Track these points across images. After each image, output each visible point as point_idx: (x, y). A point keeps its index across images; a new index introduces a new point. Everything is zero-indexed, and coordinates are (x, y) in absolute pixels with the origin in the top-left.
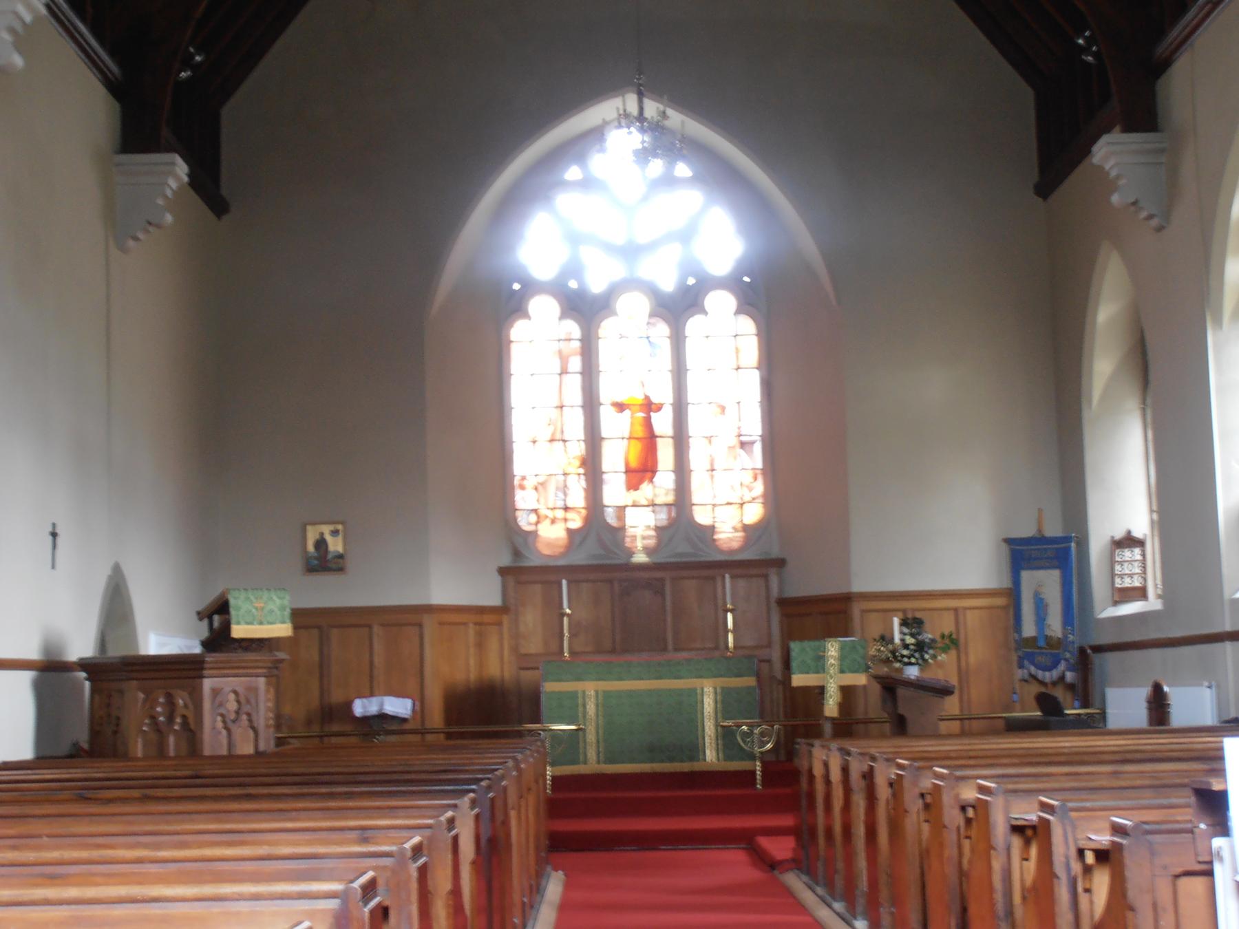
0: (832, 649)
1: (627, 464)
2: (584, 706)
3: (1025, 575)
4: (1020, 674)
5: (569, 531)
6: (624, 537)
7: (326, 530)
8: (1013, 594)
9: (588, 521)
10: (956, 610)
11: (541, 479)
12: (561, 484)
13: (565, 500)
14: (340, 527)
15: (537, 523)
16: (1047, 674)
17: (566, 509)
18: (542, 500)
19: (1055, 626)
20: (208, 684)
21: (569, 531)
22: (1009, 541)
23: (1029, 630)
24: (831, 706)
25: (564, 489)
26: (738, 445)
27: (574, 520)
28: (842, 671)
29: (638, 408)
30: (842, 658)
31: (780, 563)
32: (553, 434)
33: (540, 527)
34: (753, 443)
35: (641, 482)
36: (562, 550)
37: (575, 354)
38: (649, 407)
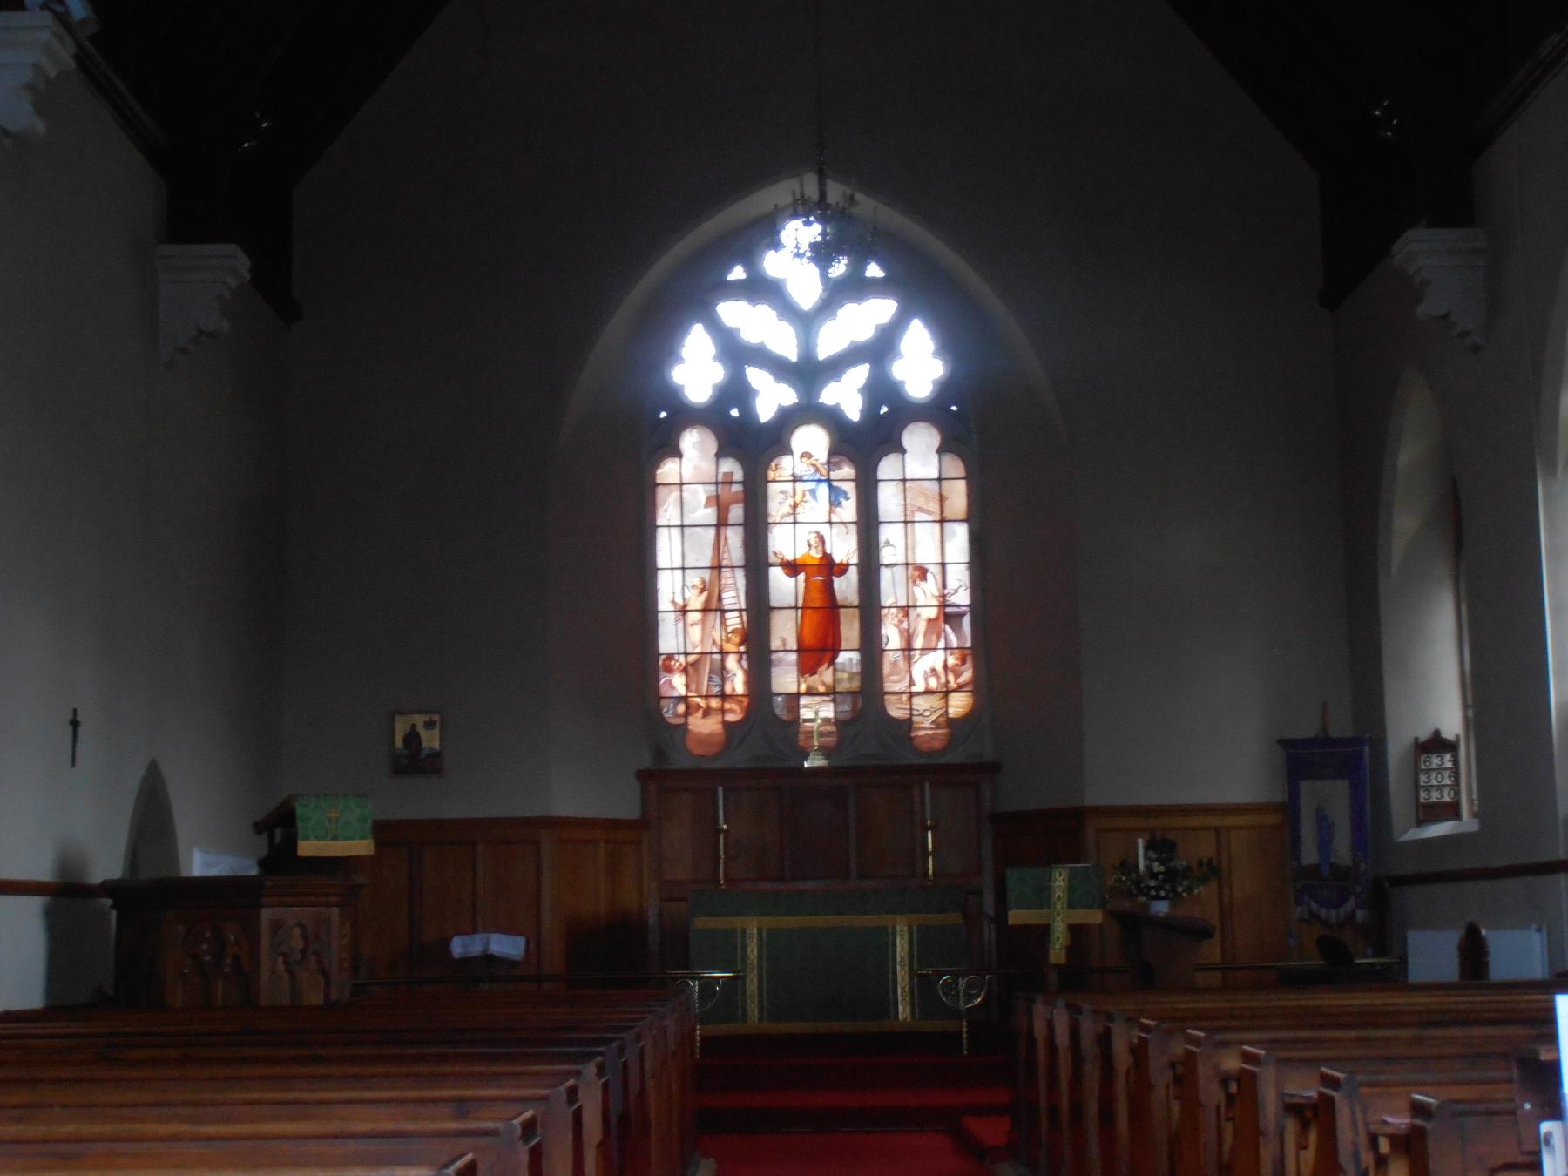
0: (1060, 880)
1: (800, 641)
2: (744, 948)
3: (1305, 786)
4: (1298, 912)
5: (726, 724)
6: (797, 733)
7: (419, 720)
8: (1289, 810)
9: (749, 712)
10: (1217, 830)
11: (691, 658)
12: (718, 665)
13: (723, 686)
14: (436, 718)
15: (687, 714)
16: (1333, 912)
17: (723, 697)
18: (693, 687)
19: (1342, 850)
20: (266, 914)
21: (726, 724)
22: (1285, 743)
23: (1310, 855)
24: (1057, 951)
25: (722, 672)
26: (942, 619)
27: (731, 711)
28: (1071, 906)
30: (1071, 889)
31: (993, 768)
32: (707, 602)
33: (691, 719)
34: (962, 615)
35: (819, 664)
37: (736, 502)
38: (830, 568)
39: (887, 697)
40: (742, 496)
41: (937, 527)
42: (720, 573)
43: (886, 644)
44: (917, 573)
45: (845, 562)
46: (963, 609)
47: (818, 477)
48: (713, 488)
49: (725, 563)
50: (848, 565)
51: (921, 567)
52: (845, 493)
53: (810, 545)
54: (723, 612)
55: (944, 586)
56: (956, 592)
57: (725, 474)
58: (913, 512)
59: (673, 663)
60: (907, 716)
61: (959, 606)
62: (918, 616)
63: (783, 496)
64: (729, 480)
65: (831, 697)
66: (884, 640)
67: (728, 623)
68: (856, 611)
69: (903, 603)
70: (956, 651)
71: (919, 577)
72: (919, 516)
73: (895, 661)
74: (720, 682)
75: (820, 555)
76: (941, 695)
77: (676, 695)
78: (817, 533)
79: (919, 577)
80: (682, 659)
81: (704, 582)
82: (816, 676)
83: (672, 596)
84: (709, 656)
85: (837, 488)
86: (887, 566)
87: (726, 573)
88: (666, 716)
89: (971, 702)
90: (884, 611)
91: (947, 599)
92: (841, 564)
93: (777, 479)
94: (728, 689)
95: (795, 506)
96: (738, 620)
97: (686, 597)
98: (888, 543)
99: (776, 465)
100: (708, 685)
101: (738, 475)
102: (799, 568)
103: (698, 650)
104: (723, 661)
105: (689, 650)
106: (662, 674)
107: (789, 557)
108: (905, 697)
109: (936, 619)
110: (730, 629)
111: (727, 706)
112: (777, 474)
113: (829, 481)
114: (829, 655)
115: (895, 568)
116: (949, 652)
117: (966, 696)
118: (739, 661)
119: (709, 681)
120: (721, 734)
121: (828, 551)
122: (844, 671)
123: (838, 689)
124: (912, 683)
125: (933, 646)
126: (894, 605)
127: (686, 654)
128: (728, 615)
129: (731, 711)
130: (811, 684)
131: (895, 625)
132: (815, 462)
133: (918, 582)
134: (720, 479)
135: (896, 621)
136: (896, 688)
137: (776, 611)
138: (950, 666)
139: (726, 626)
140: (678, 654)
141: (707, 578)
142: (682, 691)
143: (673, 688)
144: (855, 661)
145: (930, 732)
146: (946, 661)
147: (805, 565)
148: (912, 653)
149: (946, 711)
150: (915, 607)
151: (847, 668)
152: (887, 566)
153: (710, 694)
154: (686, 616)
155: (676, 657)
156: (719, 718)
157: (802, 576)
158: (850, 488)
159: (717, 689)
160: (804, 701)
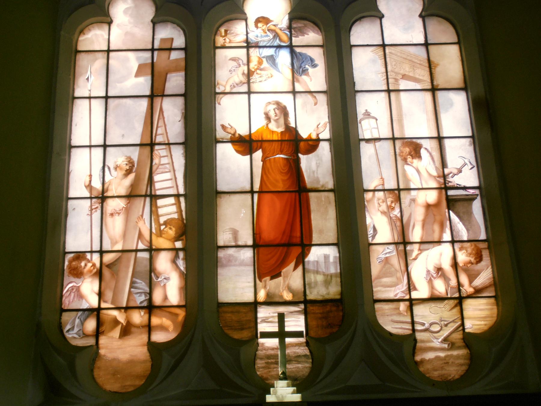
1: (256, 234)
5: (152, 346)
11: (108, 258)
13: (150, 294)
15: (98, 333)
18: (109, 295)
21: (152, 346)
26: (444, 203)
27: (162, 328)
29: (276, 146)
32: (134, 186)
33: (103, 340)
34: (470, 199)
35: (283, 263)
36: (139, 383)
37: (176, 70)
39: (377, 306)
40: (183, 64)
41: (428, 96)
42: (152, 151)
43: (374, 237)
44: (407, 150)
45: (314, 137)
46: (471, 191)
47: (277, 42)
48: (148, 55)
49: (159, 139)
50: (318, 140)
51: (412, 143)
52: (312, 60)
53: (268, 118)
54: (154, 197)
55: (444, 164)
56: (460, 171)
57: (163, 40)
58: (396, 80)
59: (83, 264)
60: (410, 332)
61: (465, 188)
62: (413, 200)
63: (234, 64)
64: (169, 47)
65: (302, 306)
66: (370, 232)
67: (161, 211)
68: (331, 195)
69: (391, 184)
70: (468, 244)
71: (410, 154)
72: (403, 84)
73: (387, 258)
74: (147, 290)
75: (281, 129)
76: (452, 303)
77: (85, 306)
78: (278, 103)
79: (410, 154)
80: (96, 258)
81: (130, 162)
82: (280, 279)
83: (88, 179)
84: (134, 254)
85: (300, 54)
86: (368, 141)
87: (159, 151)
88: (68, 336)
89: (495, 311)
90: (368, 196)
91: (450, 179)
92: (309, 139)
93: (227, 45)
94: (157, 299)
95: (249, 74)
96: (174, 209)
97: (107, 179)
98: (367, 115)
99: (226, 31)
100: (130, 293)
101: (179, 41)
102: (255, 145)
103: (119, 247)
104: (151, 260)
105: (107, 246)
106: (67, 279)
107: (243, 131)
108: (403, 306)
109: (437, 205)
110: (162, 220)
111: (155, 321)
112: (227, 40)
113: (291, 47)
114: (296, 251)
115: (378, 144)
116: (457, 246)
117: (487, 304)
118: (174, 262)
119: (131, 287)
120: (144, 362)
121: (293, 125)
122: (317, 272)
123: (311, 296)
124: (411, 287)
125: (436, 239)
126: (380, 187)
127: (101, 252)
128: (160, 202)
129: (162, 328)
130: (272, 290)
131: (383, 213)
132: (273, 28)
133: (409, 159)
134: (156, 46)
135: (384, 207)
136: (391, 295)
137: (222, 195)
138: (461, 264)
139: (158, 216)
140: (92, 252)
141: (135, 158)
142: (93, 301)
143: (81, 296)
144: (331, 259)
145: (442, 354)
146: (455, 258)
147: (262, 141)
148: (408, 248)
149: (463, 324)
150: (410, 189)
151: (322, 268)
152: (368, 141)
153: (132, 304)
154: (105, 204)
155: (88, 256)
156: (145, 338)
157: (258, 155)
158: (317, 55)
159: (143, 298)
160: (263, 312)
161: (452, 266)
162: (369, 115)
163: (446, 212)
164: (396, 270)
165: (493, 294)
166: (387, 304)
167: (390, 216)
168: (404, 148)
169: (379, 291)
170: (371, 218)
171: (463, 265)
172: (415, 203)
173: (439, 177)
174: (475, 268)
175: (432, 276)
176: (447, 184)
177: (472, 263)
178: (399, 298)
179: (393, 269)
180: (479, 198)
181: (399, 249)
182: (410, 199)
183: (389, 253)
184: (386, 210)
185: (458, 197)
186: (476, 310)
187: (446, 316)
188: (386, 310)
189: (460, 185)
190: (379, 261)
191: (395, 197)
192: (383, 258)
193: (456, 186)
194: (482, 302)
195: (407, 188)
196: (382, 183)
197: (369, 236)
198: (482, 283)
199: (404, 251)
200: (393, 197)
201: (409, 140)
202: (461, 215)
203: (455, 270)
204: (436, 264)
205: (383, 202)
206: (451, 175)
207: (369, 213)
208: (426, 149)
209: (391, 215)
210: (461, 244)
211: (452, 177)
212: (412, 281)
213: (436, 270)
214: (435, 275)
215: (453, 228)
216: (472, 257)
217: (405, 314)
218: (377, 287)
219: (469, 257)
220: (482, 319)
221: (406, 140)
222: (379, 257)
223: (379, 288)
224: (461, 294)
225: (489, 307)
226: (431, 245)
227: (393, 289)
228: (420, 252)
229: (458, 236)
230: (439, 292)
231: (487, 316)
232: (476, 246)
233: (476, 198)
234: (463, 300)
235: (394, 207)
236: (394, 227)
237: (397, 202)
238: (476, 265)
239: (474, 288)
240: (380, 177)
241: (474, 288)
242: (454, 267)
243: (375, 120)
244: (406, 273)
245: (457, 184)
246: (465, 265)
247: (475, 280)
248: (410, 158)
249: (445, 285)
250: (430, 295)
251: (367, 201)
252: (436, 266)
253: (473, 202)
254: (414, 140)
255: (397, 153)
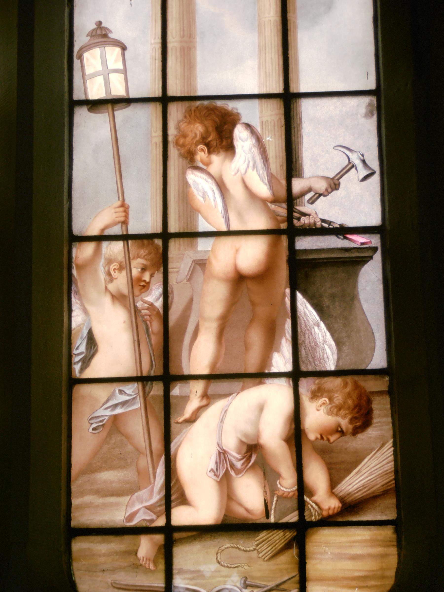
51: (214, 109)
70: (338, 381)
73: (115, 418)
91: (306, 208)
117: (373, 542)
125: (252, 369)
126: (117, 230)
138: (312, 436)
161: (287, 440)
162: (105, 36)
163: (284, 295)
164: (137, 449)
165: (391, 515)
166: (104, 542)
167: (135, 307)
168: (189, 123)
169: (89, 506)
170: (86, 312)
171: (319, 436)
172: (204, 272)
173: (275, 201)
174: (348, 445)
175: (232, 466)
176: (295, 221)
177: (342, 433)
178: (139, 525)
179: (130, 448)
180: (378, 256)
181: (152, 393)
182: (194, 261)
183: (124, 404)
184: (125, 290)
185: (323, 256)
186: (341, 557)
187: (259, 574)
188: (100, 556)
189: (330, 223)
190: (94, 425)
191: (152, 255)
192: (107, 418)
193: (319, 224)
194: (359, 538)
195: (189, 231)
196: (122, 219)
197: (76, 359)
198: (364, 486)
199: (162, 399)
200: (149, 257)
201: (206, 103)
202: (326, 302)
203: (294, 449)
204: (246, 436)
205: (121, 268)
206: (308, 197)
207: (80, 299)
208: (248, 126)
209: (139, 304)
210: (317, 380)
211: (312, 201)
212: (178, 480)
213: (244, 449)
214: (239, 465)
215: (301, 339)
216: (344, 417)
217: (152, 567)
218: (82, 494)
219: (337, 415)
220: (354, 583)
221: (198, 103)
222: (97, 414)
223: (88, 499)
224: (306, 513)
225: (379, 550)
226: (237, 384)
227: (125, 499)
228: (205, 402)
229: (311, 360)
230: (247, 510)
231: (371, 574)
232: (356, 386)
233: (371, 258)
234: (310, 531)
235: (148, 283)
236: (143, 336)
237: (158, 270)
238: (353, 437)
239: (342, 500)
240: (119, 203)
241: (342, 500)
242: (293, 443)
243: (118, 50)
244: (163, 458)
245: (323, 221)
246: (322, 438)
247: (348, 478)
248: (202, 150)
249: (265, 492)
250: (222, 516)
251: (79, 267)
252: (244, 440)
253: (360, 269)
254: (219, 103)
255: (171, 138)
